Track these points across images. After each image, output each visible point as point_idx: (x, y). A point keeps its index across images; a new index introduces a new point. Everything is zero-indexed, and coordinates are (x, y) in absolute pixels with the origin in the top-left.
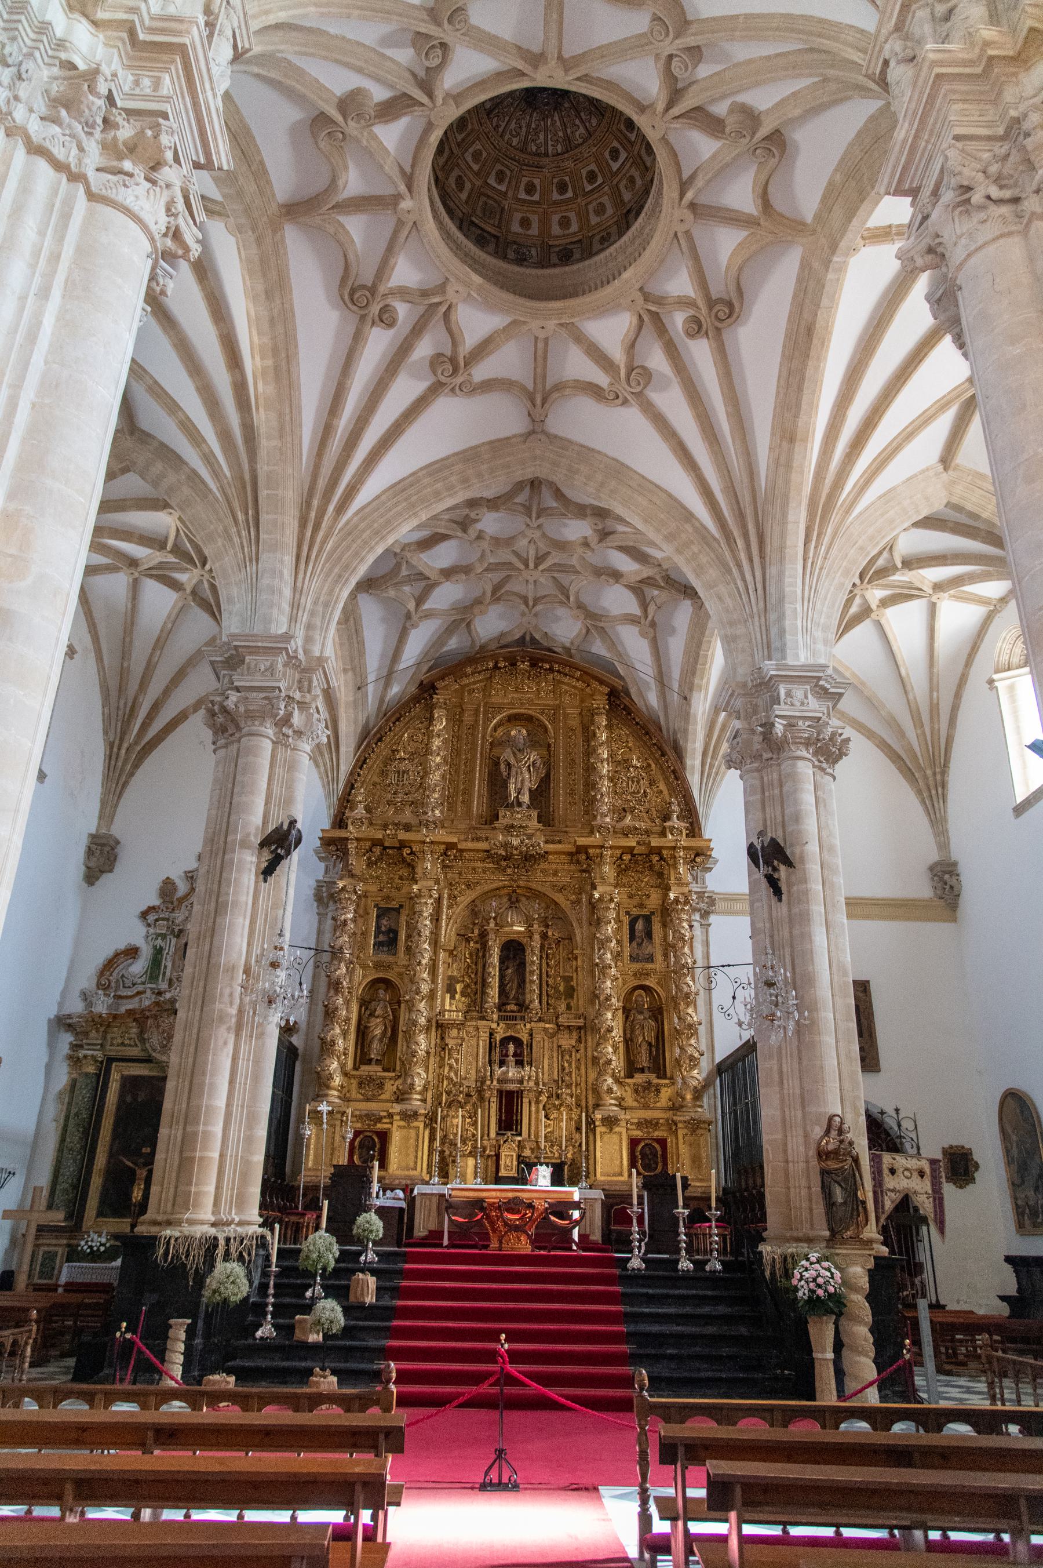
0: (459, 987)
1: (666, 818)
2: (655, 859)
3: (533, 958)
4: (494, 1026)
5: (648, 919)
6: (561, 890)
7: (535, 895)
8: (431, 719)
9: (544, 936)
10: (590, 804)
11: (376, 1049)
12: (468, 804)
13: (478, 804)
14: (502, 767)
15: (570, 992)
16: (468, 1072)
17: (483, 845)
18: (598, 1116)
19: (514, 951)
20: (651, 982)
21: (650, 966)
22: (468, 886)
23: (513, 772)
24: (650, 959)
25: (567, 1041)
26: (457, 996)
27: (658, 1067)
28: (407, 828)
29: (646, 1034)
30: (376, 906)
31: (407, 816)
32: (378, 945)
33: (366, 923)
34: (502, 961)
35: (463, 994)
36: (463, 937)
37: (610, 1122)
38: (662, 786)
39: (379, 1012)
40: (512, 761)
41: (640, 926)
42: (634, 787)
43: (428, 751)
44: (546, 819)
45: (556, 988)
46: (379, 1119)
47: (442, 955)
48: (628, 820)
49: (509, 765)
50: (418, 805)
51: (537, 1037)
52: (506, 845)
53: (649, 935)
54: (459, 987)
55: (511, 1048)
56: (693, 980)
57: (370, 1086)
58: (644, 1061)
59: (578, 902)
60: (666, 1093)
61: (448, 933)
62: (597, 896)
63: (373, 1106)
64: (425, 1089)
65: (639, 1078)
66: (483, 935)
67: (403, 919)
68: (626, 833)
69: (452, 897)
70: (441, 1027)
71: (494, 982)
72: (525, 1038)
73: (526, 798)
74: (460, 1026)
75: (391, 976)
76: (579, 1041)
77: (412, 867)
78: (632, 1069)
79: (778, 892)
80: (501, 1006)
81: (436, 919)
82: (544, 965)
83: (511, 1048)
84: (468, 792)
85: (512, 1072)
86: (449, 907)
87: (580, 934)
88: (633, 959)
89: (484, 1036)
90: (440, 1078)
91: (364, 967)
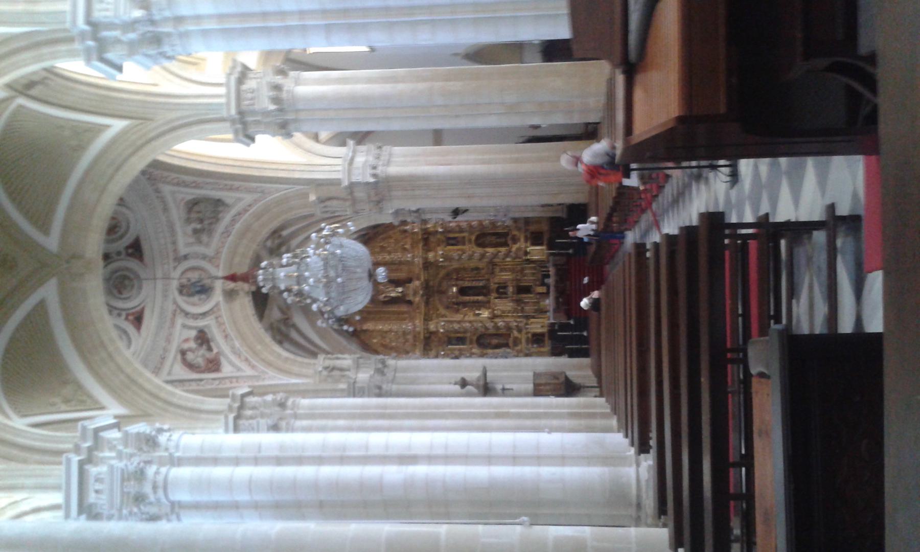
0: (477, 312)
1: (405, 231)
2: (426, 236)
3: (467, 284)
4: (492, 297)
5: (449, 239)
6: (438, 274)
7: (440, 284)
8: (365, 331)
9: (457, 279)
10: (401, 263)
11: (502, 341)
12: (403, 313)
13: (404, 308)
14: (386, 299)
15: (477, 269)
16: (509, 306)
17: (423, 306)
18: (524, 258)
19: (463, 291)
20: (473, 238)
21: (466, 239)
22: (438, 310)
23: (388, 295)
24: (464, 237)
25: (497, 270)
26: (480, 312)
27: (505, 235)
28: (415, 337)
29: (493, 239)
30: (447, 346)
31: (410, 337)
32: (463, 344)
33: (455, 349)
34: (468, 296)
35: (479, 310)
36: (457, 311)
37: (526, 253)
38: (391, 232)
39: (488, 341)
40: (383, 295)
41: (453, 242)
42: (393, 245)
43: (380, 331)
44: (410, 280)
45: (477, 274)
46: (528, 338)
47: (466, 318)
48: (407, 246)
49: (385, 297)
50: (405, 333)
51: (496, 281)
52: (422, 296)
53: (455, 238)
54: (477, 312)
55: (501, 290)
56: (473, 221)
57: (517, 342)
58: (503, 240)
59: (442, 266)
60: (515, 233)
61: (459, 317)
62: (441, 260)
63: (523, 341)
64: (516, 322)
65: (510, 242)
66: (458, 304)
67: (453, 335)
68: (412, 247)
69: (443, 316)
70: (493, 317)
71: (476, 298)
72: (497, 286)
73: (400, 289)
74: (494, 310)
75: (475, 338)
76: (496, 265)
77: (432, 333)
78: (505, 244)
79: (466, 211)
80: (485, 295)
81: (451, 322)
82: (468, 279)
83: (501, 290)
84: (399, 313)
85: (511, 289)
86: (446, 317)
87: (455, 265)
88: (464, 244)
89: (496, 300)
90: (513, 316)
91: (471, 349)
